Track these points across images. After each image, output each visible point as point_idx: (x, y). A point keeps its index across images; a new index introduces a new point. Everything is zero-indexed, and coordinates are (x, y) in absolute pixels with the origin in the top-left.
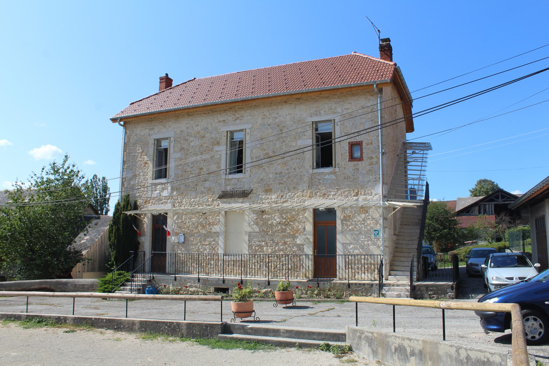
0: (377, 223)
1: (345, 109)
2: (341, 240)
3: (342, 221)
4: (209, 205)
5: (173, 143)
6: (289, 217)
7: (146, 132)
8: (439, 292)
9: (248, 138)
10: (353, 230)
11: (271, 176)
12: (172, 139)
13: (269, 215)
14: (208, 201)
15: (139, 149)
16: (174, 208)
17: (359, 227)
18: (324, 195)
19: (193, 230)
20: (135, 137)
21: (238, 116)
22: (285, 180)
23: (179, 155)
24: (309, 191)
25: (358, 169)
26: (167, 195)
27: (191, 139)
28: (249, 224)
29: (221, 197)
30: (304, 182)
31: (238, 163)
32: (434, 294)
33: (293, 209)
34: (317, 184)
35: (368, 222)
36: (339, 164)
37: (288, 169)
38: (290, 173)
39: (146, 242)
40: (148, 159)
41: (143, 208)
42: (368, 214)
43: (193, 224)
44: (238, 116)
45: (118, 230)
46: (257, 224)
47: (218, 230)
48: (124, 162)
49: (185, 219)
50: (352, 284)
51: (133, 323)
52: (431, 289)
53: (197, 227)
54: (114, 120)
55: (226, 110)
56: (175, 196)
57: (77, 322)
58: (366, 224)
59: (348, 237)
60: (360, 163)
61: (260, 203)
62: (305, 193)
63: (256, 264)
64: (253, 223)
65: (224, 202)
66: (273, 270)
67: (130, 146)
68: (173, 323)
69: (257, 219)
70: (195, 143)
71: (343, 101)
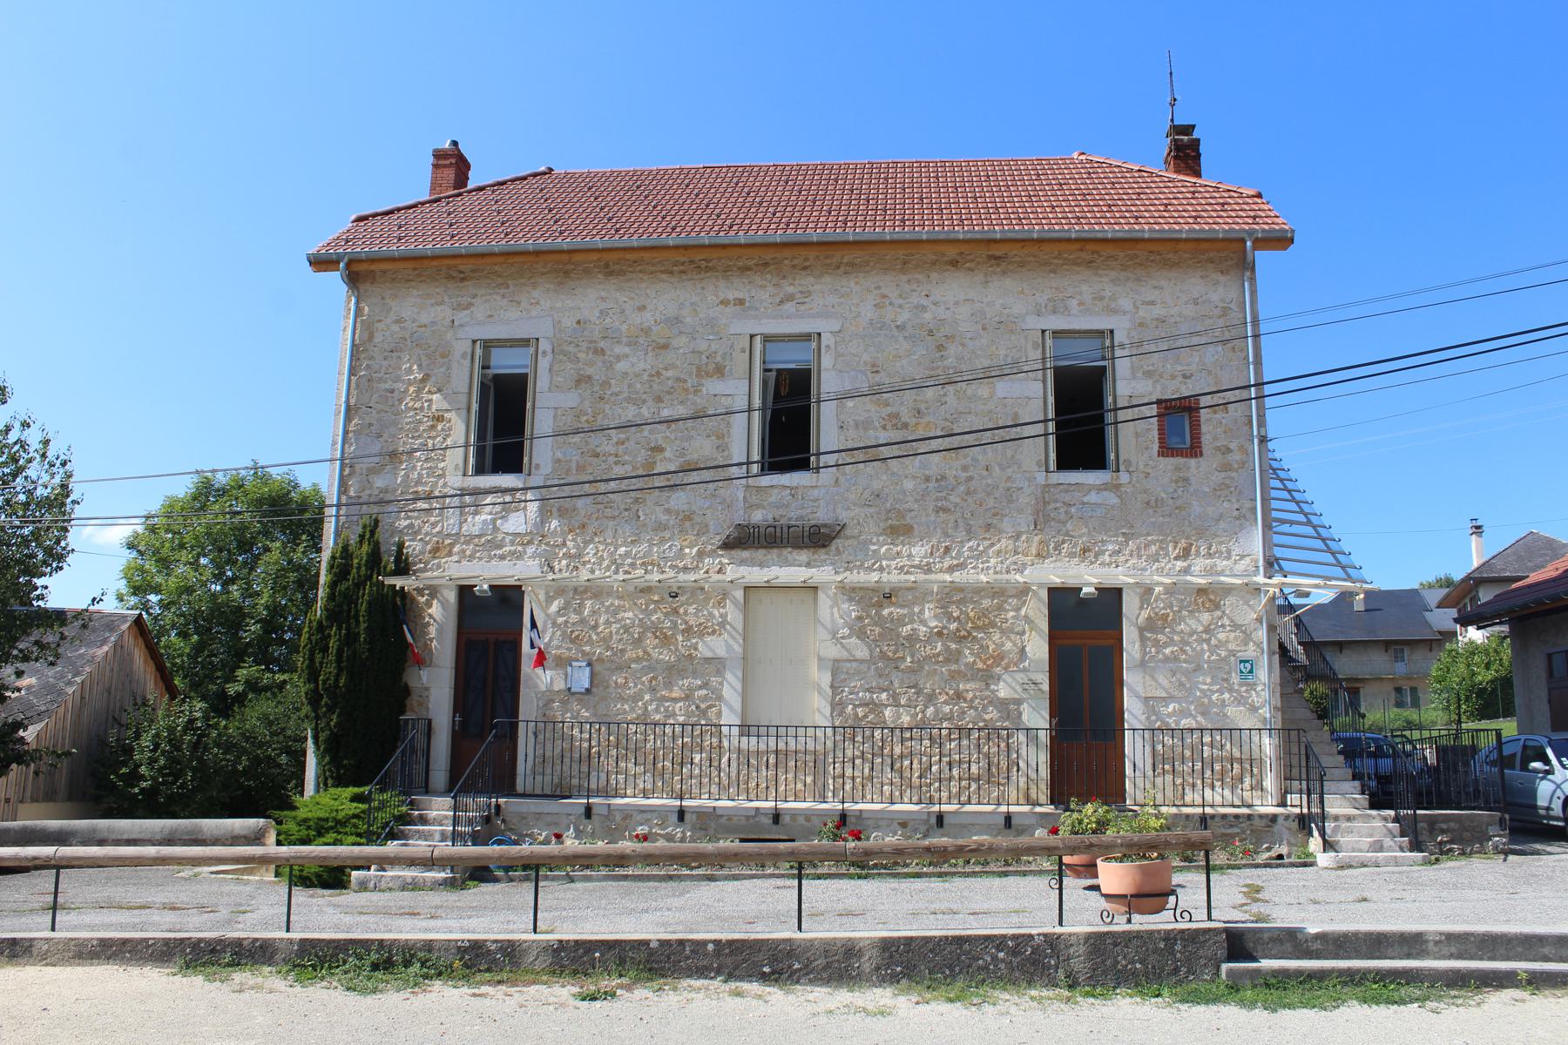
0: (1247, 638)
1: (1144, 303)
2: (1140, 689)
3: (1141, 630)
4: (685, 569)
5: (549, 357)
7: (443, 313)
8: (1467, 835)
9: (827, 361)
10: (1176, 659)
11: (909, 485)
12: (544, 345)
13: (902, 607)
14: (680, 555)
15: (410, 371)
16: (550, 576)
17: (1194, 650)
18: (1085, 550)
20: (396, 328)
21: (791, 289)
22: (958, 500)
23: (570, 399)
24: (1037, 539)
25: (1186, 480)
26: (522, 529)
27: (618, 350)
28: (834, 634)
29: (728, 545)
30: (1020, 511)
31: (788, 436)
32: (1451, 842)
33: (980, 590)
34: (1062, 516)
35: (1222, 636)
37: (965, 468)
38: (970, 479)
39: (436, 688)
40: (446, 406)
41: (424, 570)
43: (627, 629)
44: (791, 289)
45: (350, 639)
46: (861, 634)
47: (721, 652)
50: (1213, 817)
51: (850, 950)
52: (1444, 826)
53: (638, 642)
54: (320, 263)
55: (748, 269)
56: (554, 533)
57: (573, 960)
58: (1213, 641)
59: (1161, 679)
60: (1193, 462)
61: (870, 569)
62: (1022, 545)
63: (858, 762)
64: (846, 631)
65: (742, 562)
67: (372, 358)
68: (1031, 936)
69: (859, 618)
70: (635, 363)
71: (1138, 280)
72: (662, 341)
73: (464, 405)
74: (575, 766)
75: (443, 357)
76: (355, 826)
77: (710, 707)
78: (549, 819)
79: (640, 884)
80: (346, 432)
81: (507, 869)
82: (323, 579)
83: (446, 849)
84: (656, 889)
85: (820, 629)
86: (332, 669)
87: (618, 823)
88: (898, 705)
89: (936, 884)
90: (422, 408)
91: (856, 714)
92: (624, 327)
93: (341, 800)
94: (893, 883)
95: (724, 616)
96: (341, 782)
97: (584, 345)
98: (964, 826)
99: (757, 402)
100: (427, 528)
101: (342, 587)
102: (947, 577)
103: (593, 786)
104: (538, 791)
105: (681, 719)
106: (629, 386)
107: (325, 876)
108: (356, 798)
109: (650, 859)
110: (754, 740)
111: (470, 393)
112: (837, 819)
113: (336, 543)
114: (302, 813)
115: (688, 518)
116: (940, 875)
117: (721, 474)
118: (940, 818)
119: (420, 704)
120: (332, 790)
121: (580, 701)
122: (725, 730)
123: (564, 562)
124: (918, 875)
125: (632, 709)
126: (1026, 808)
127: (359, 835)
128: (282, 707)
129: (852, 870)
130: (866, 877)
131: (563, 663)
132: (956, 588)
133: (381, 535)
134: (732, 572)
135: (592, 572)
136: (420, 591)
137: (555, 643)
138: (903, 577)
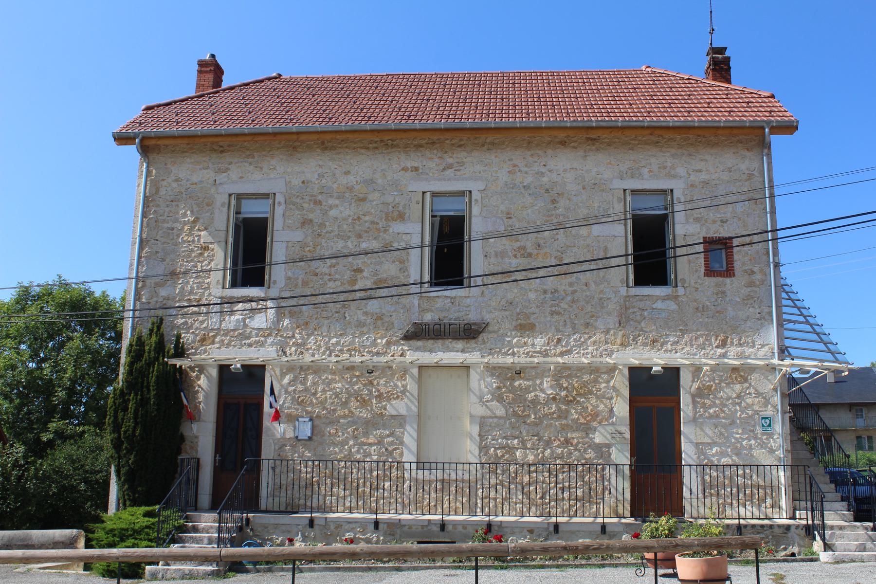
0: (767, 402)
1: (694, 171)
2: (692, 437)
3: (693, 396)
4: (378, 354)
5: (283, 207)
6: (578, 384)
7: (208, 175)
9: (475, 210)
10: (718, 416)
11: (532, 296)
12: (279, 198)
13: (528, 380)
15: (185, 215)
16: (285, 359)
17: (730, 410)
18: (654, 341)
19: (334, 411)
20: (175, 185)
21: (450, 161)
22: (566, 306)
23: (298, 236)
24: (621, 333)
25: (724, 292)
26: (264, 326)
27: (331, 201)
28: (481, 398)
29: (407, 337)
30: (609, 314)
33: (581, 368)
34: (638, 318)
35: (749, 401)
36: (683, 280)
37: (571, 285)
38: (574, 292)
39: (203, 437)
40: (210, 239)
41: (195, 354)
42: (747, 385)
43: (337, 395)
44: (450, 161)
45: (143, 402)
46: (500, 399)
47: (403, 411)
48: (142, 243)
49: (314, 384)
50: (746, 526)
53: (345, 404)
54: (122, 139)
55: (421, 146)
56: (287, 329)
58: (743, 404)
59: (708, 430)
60: (728, 280)
61: (506, 354)
64: (489, 397)
65: (418, 349)
66: (539, 501)
67: (158, 206)
69: (499, 388)
70: (342, 211)
71: (690, 155)
72: (361, 196)
73: (223, 239)
75: (208, 205)
76: (148, 534)
77: (395, 449)
78: (284, 528)
80: (140, 257)
81: (255, 563)
82: (123, 360)
83: (212, 549)
84: (362, 577)
85: (472, 396)
86: (131, 423)
87: (333, 530)
88: (526, 448)
89: (556, 572)
90: (193, 241)
91: (496, 455)
92: (335, 185)
93: (137, 516)
96: (136, 503)
97: (307, 198)
98: (573, 533)
99: (427, 239)
100: (197, 324)
101: (138, 365)
102: (560, 360)
105: (375, 458)
106: (339, 226)
107: (126, 569)
108: (147, 514)
111: (227, 231)
112: (485, 527)
113: (132, 335)
114: (109, 525)
116: (558, 567)
117: (403, 290)
118: (556, 526)
119: (192, 448)
120: (130, 509)
121: (304, 446)
122: (407, 466)
123: (293, 349)
124: (543, 567)
125: (341, 451)
126: (615, 520)
127: (150, 540)
128: (94, 450)
129: (496, 563)
130: (506, 568)
131: (292, 419)
132: (565, 367)
133: (165, 329)
134: (410, 356)
135: (313, 355)
136: (192, 369)
137: (287, 405)
138: (529, 359)
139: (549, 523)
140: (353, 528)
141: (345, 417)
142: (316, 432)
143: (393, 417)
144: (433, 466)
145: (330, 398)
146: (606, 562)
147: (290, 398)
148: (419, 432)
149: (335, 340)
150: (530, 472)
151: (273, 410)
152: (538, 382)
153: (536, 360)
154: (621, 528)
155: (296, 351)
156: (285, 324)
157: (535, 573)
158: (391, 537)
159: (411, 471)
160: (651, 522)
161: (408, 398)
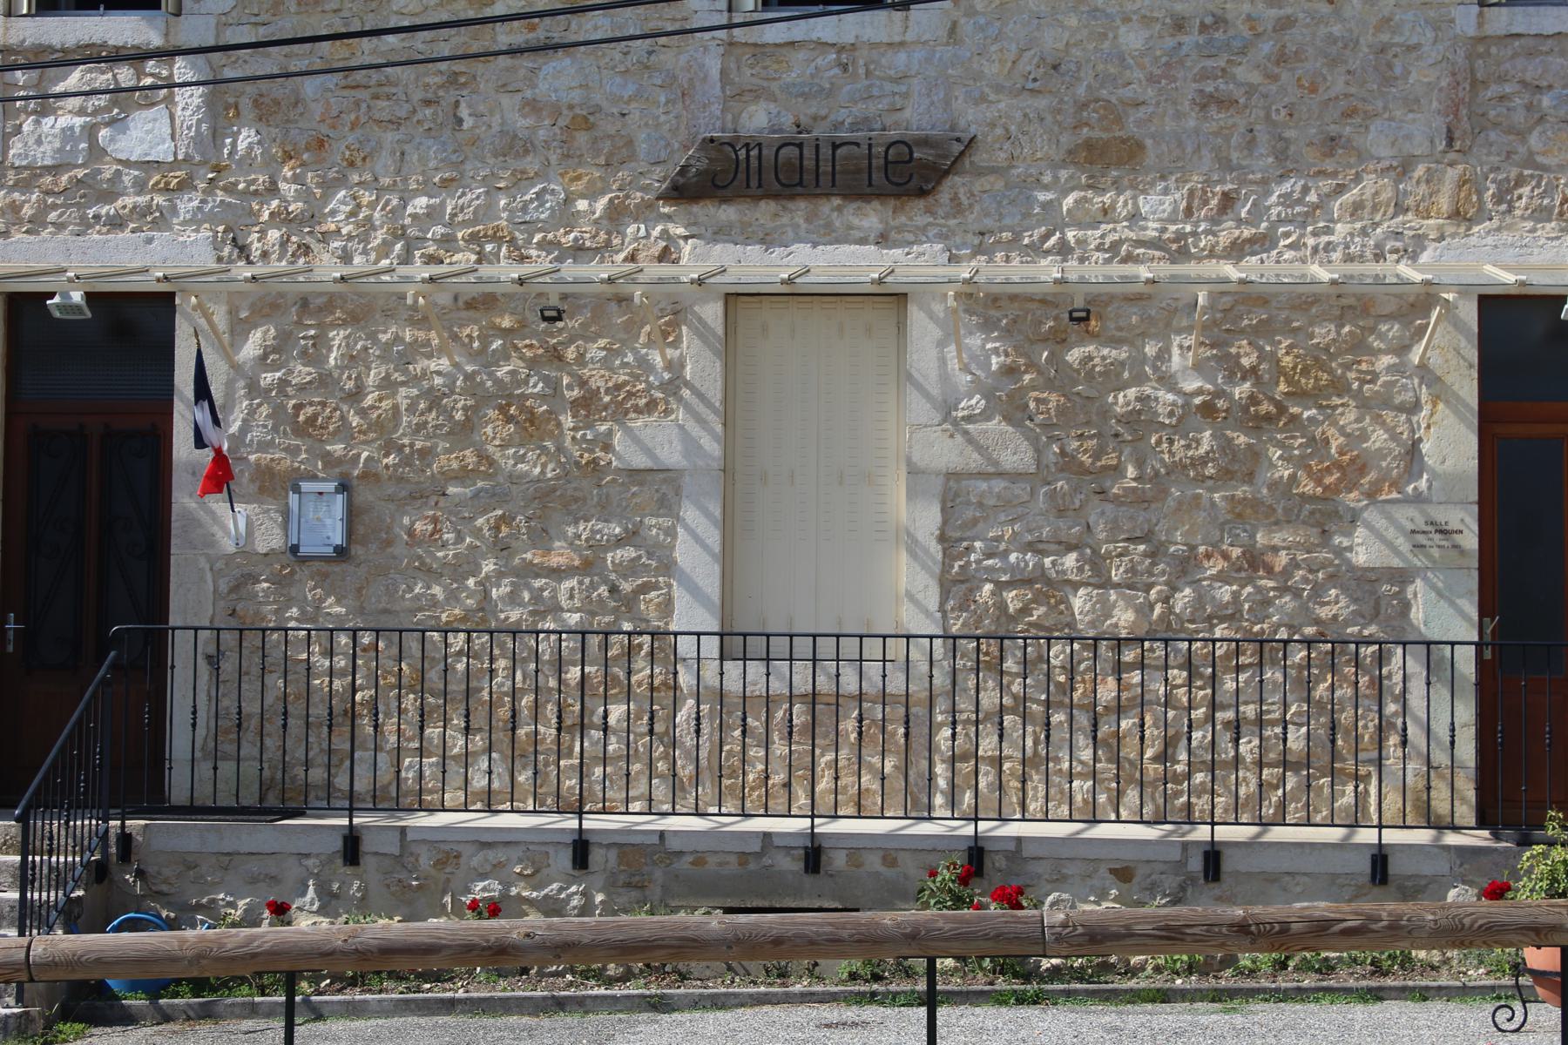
4: (578, 251)
6: (1291, 356)
13: (1115, 342)
14: (566, 216)
16: (243, 271)
22: (1255, 78)
24: (1452, 174)
26: (163, 151)
28: (947, 409)
29: (684, 191)
30: (1412, 104)
33: (1307, 301)
34: (1519, 117)
38: (1285, 24)
43: (435, 399)
46: (1014, 410)
47: (671, 455)
49: (351, 359)
53: (464, 431)
56: (247, 162)
61: (1037, 250)
62: (1415, 189)
64: (977, 402)
65: (720, 234)
69: (1010, 371)
74: (318, 738)
78: (254, 867)
79: (488, 1021)
81: (155, 989)
88: (1106, 584)
89: (1209, 1017)
91: (1002, 606)
94: (1102, 1017)
95: (675, 367)
98: (1272, 879)
102: (1231, 271)
103: (362, 785)
104: (225, 800)
105: (573, 619)
109: (501, 958)
110: (755, 669)
115: (584, 123)
116: (1217, 996)
118: (1213, 856)
122: (686, 646)
123: (274, 235)
124: (1164, 996)
125: (452, 597)
126: (1423, 836)
129: (1001, 984)
130: (1036, 1000)
131: (276, 485)
132: (1248, 296)
134: (694, 259)
135: (346, 258)
137: (255, 434)
138: (1118, 270)
139: (1185, 846)
140: (498, 866)
141: (463, 475)
142: (361, 530)
143: (635, 474)
144: (779, 646)
145: (411, 409)
146: (1389, 982)
147: (265, 410)
148: (728, 525)
149: (422, 201)
150: (1119, 669)
151: (207, 455)
152: (1150, 350)
153: (1144, 272)
154: (1442, 866)
155: (284, 243)
156: (242, 146)
157: (1136, 1018)
158: (635, 894)
159: (700, 664)
160: (1551, 843)
161: (689, 408)
